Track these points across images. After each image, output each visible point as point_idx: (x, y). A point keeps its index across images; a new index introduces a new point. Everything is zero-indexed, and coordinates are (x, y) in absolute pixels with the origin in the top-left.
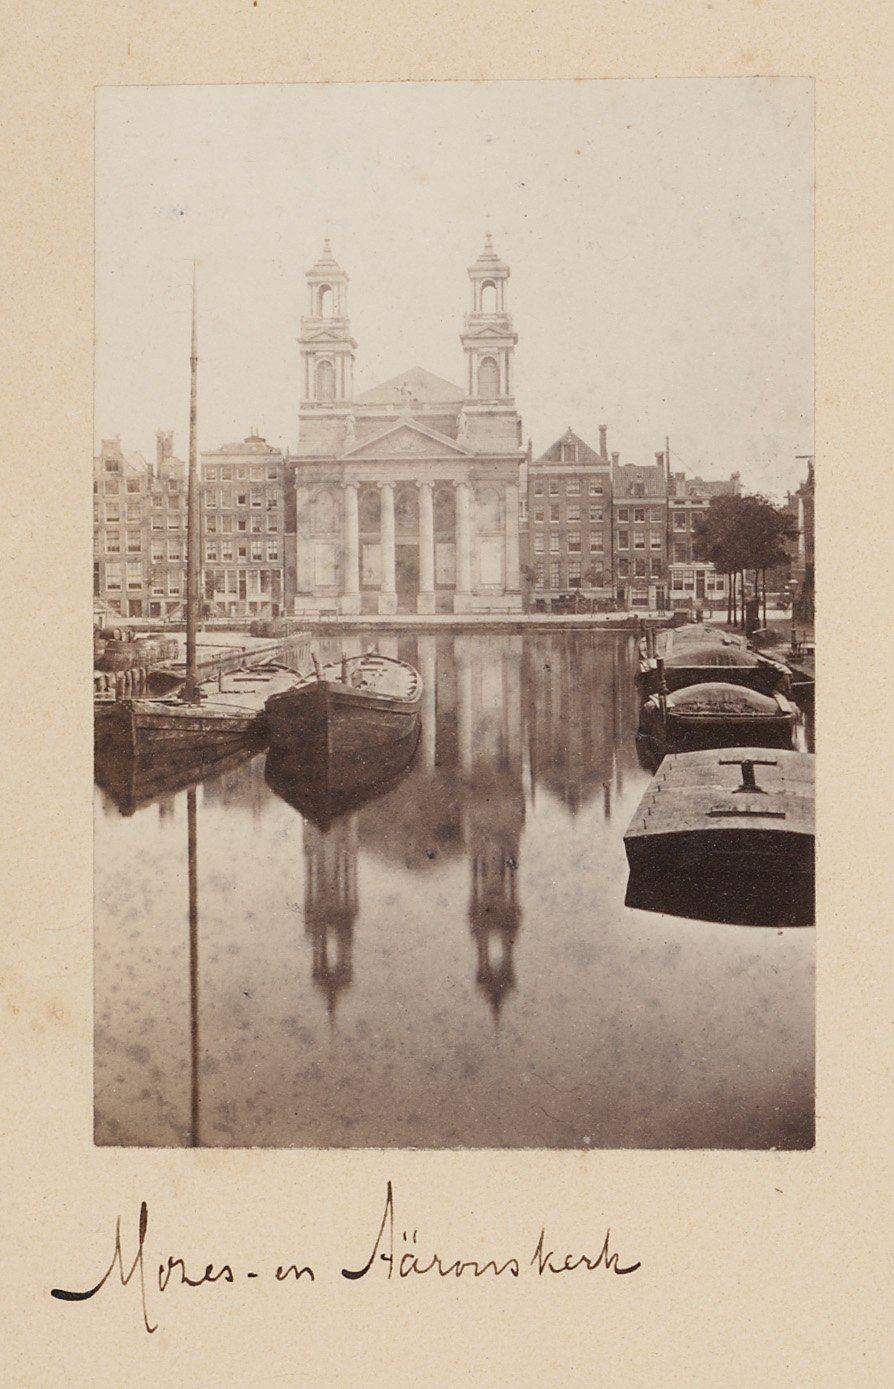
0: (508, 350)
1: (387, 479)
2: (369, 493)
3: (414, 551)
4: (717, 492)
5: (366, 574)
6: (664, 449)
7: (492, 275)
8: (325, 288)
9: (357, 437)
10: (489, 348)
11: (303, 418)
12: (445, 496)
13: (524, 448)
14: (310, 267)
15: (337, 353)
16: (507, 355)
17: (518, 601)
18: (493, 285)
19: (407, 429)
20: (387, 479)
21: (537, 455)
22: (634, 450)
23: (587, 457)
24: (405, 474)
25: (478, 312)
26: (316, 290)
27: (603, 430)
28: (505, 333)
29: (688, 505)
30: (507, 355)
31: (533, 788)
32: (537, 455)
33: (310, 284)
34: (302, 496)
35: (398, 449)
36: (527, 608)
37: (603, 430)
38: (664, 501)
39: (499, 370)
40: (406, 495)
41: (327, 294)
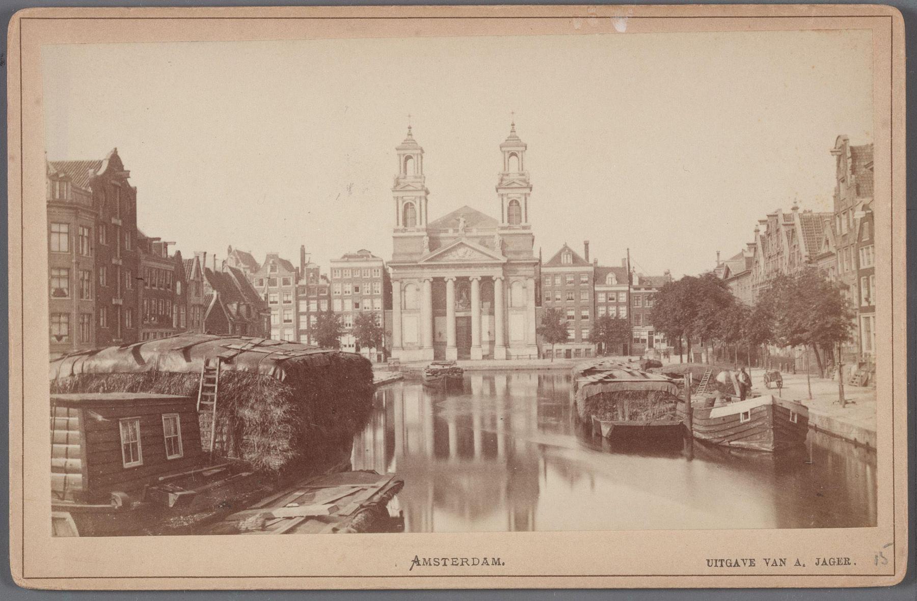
0: (526, 196)
1: (450, 275)
2: (438, 285)
3: (469, 319)
4: (661, 284)
5: (437, 335)
8: (408, 158)
9: (431, 249)
12: (487, 283)
13: (536, 255)
14: (398, 144)
15: (416, 197)
16: (526, 199)
18: (516, 155)
20: (450, 275)
21: (545, 260)
22: (608, 258)
23: (576, 260)
24: (463, 273)
25: (506, 172)
26: (403, 159)
27: (587, 244)
28: (524, 185)
29: (643, 290)
30: (526, 199)
31: (545, 468)
33: (399, 155)
34: (396, 286)
35: (457, 258)
37: (587, 244)
38: (627, 288)
39: (520, 209)
40: (463, 284)
41: (410, 162)
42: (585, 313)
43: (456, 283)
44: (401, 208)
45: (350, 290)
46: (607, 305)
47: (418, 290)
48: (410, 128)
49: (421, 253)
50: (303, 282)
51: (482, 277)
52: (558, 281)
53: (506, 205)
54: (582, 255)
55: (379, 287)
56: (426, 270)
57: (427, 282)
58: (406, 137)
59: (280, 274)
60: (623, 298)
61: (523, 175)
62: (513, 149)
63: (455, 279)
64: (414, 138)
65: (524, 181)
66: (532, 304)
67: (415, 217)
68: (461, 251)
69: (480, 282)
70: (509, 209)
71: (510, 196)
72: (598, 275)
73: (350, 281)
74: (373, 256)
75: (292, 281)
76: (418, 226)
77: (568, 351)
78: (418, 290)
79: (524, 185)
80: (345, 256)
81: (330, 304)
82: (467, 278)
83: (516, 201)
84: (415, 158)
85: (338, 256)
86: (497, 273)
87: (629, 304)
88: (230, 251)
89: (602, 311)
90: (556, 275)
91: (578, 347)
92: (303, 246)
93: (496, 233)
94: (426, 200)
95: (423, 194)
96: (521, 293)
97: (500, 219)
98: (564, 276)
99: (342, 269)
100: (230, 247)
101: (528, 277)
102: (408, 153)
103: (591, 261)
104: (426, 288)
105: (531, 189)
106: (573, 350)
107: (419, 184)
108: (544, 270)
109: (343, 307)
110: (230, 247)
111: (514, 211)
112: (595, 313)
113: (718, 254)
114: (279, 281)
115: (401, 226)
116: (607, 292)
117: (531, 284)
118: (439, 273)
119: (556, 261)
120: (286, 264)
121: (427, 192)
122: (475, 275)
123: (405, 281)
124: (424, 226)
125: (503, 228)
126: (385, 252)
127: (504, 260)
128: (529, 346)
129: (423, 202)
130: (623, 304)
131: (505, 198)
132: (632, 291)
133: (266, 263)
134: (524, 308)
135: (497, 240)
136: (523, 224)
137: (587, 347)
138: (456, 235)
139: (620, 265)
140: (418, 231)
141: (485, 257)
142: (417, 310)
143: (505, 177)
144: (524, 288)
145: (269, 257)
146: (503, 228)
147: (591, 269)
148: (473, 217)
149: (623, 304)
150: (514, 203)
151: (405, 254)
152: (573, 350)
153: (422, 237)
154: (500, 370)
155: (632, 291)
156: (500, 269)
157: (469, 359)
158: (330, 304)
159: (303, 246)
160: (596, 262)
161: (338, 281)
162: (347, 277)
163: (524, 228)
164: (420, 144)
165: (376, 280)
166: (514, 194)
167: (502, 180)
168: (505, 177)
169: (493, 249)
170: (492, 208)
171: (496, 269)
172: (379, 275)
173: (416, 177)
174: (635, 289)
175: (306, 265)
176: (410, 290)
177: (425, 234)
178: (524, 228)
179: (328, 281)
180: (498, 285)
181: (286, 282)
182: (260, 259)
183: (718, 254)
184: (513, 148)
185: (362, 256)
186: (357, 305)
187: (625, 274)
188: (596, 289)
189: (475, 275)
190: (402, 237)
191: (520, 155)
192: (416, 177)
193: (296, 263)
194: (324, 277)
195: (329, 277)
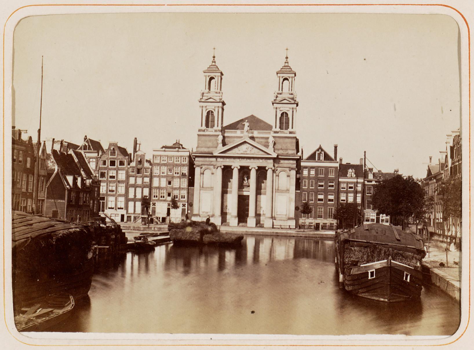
1: (236, 165)
2: (227, 171)
6: (363, 157)
7: (286, 74)
8: (212, 78)
10: (285, 108)
11: (198, 135)
12: (262, 172)
17: (293, 223)
18: (288, 80)
19: (245, 142)
20: (236, 165)
21: (305, 157)
23: (327, 158)
24: (245, 163)
25: (280, 92)
27: (336, 147)
28: (293, 102)
32: (305, 157)
34: (197, 171)
36: (299, 226)
37: (336, 147)
38: (362, 181)
40: (244, 171)
41: (213, 81)
42: (331, 197)
43: (240, 170)
44: (205, 114)
45: (165, 171)
46: (347, 192)
47: (213, 174)
48: (214, 57)
49: (216, 147)
50: (133, 164)
51: (259, 167)
52: (313, 172)
53: (279, 116)
54: (332, 155)
55: (186, 170)
56: (219, 159)
57: (219, 168)
58: (211, 63)
59: (118, 157)
60: (359, 188)
61: (292, 94)
62: (286, 76)
63: (239, 168)
64: (217, 64)
65: (293, 99)
66: (294, 188)
67: (214, 122)
68: (244, 147)
69: (257, 171)
70: (281, 119)
71: (281, 109)
72: (343, 169)
73: (165, 165)
74: (183, 148)
75: (126, 163)
76: (215, 127)
77: (318, 225)
78: (213, 174)
79: (293, 102)
80: (163, 147)
81: (151, 181)
82: (247, 167)
83: (286, 113)
84: (216, 79)
85: (159, 147)
86: (269, 164)
87: (363, 192)
88: (85, 139)
89: (343, 197)
90: (313, 167)
91: (325, 221)
92: (136, 138)
93: (271, 136)
94: (223, 109)
95: (220, 104)
96: (285, 180)
97: (274, 127)
98: (316, 168)
99: (161, 156)
100: (86, 136)
101: (291, 169)
102: (212, 75)
103: (338, 160)
104: (219, 173)
105: (297, 105)
106: (321, 224)
107: (219, 98)
108: (303, 164)
109: (160, 184)
110: (86, 136)
111: (284, 121)
112: (338, 198)
113: (431, 159)
114: (117, 163)
115: (204, 127)
116: (348, 183)
117: (293, 173)
118: (228, 162)
119: (312, 157)
120: (123, 151)
121: (224, 104)
122: (253, 165)
123: (204, 167)
124: (220, 128)
125: (275, 132)
126: (191, 145)
127: (275, 155)
128: (290, 219)
129: (220, 110)
130: (360, 192)
131: (278, 110)
132: (366, 183)
133: (109, 148)
134: (288, 191)
135: (271, 140)
136: (290, 129)
137: (332, 222)
138: (242, 135)
139: (357, 163)
140: (216, 131)
141: (261, 153)
142: (212, 188)
143: (278, 95)
144: (288, 176)
145: (110, 145)
146: (275, 132)
147: (337, 165)
148: (255, 123)
149: (360, 192)
150: (284, 115)
151: (205, 147)
152: (321, 224)
153: (218, 135)
154: (266, 235)
155: (366, 183)
156: (272, 161)
157: (246, 226)
158: (151, 181)
159: (136, 138)
160: (341, 160)
161: (158, 164)
162: (164, 162)
163: (290, 133)
164: (221, 69)
165: (184, 165)
166: (285, 108)
167: (277, 97)
168: (278, 95)
169: (267, 146)
170: (269, 116)
171: (269, 161)
172: (187, 162)
173: (216, 93)
174: (368, 181)
175: (136, 152)
176: (207, 173)
177: (220, 133)
178: (290, 133)
179: (151, 164)
180: (269, 173)
181: (122, 163)
182: (105, 147)
183: (431, 159)
184: (286, 74)
185: (175, 148)
186: (170, 183)
187: (360, 171)
188: (340, 180)
189: (253, 165)
190: (204, 135)
191: (290, 80)
192: (216, 93)
193: (130, 150)
194: (149, 161)
195: (152, 162)
